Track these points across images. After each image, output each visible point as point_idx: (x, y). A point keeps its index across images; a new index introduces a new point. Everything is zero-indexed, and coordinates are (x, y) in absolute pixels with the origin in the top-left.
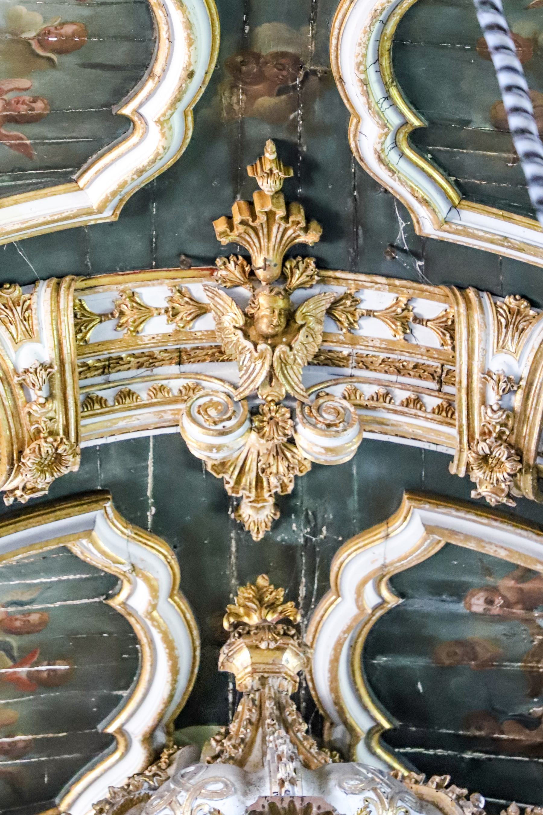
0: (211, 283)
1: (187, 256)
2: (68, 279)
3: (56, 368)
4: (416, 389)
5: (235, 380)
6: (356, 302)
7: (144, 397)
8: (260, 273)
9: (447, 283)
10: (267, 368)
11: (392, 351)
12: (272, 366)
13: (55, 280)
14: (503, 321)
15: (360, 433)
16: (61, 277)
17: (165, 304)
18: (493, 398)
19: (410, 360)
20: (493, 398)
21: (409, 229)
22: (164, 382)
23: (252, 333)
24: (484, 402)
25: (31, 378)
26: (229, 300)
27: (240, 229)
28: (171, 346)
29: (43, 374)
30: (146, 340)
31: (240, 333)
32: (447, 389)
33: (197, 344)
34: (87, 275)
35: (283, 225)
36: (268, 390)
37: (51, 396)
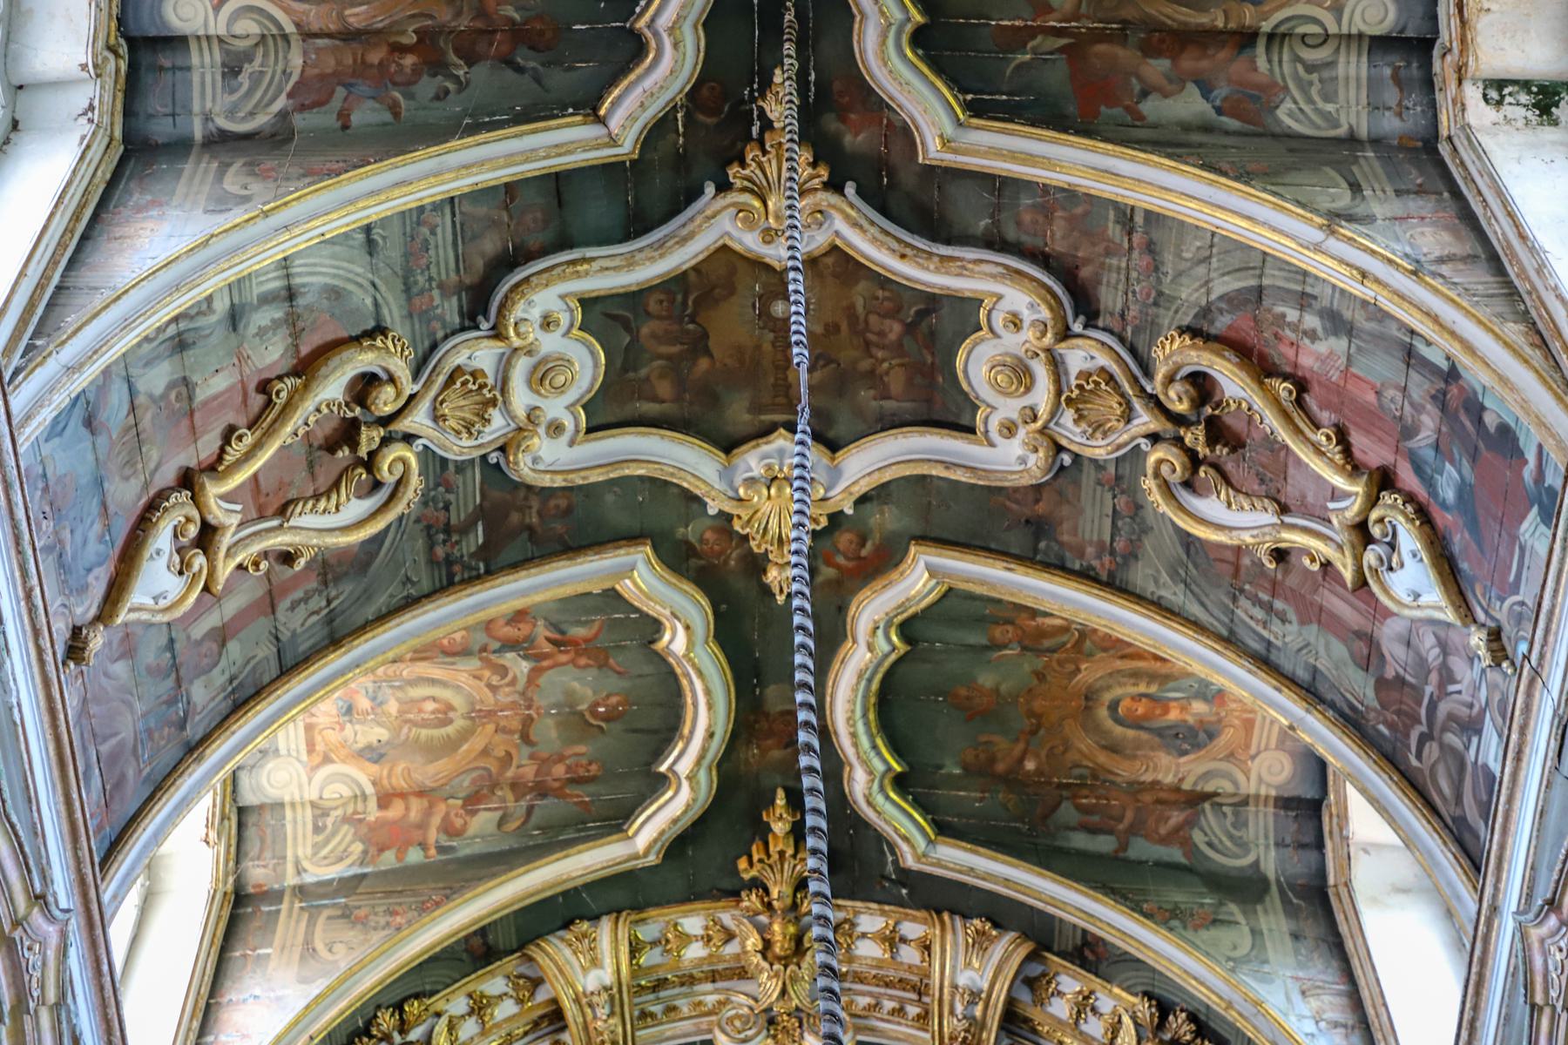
0: (737, 912)
1: (718, 890)
2: (624, 914)
3: (615, 990)
4: (902, 1001)
5: (756, 994)
6: (853, 925)
7: (685, 1010)
8: (775, 903)
9: (927, 908)
10: (780, 983)
11: (880, 968)
12: (784, 984)
13: (615, 915)
14: (970, 940)
15: (854, 1037)
16: (619, 912)
17: (700, 932)
18: (959, 1008)
19: (892, 974)
20: (959, 1008)
21: (896, 862)
22: (702, 998)
23: (769, 955)
24: (952, 1012)
25: (595, 999)
26: (750, 927)
27: (758, 866)
28: (706, 968)
29: (605, 996)
30: (686, 963)
31: (759, 956)
32: (926, 999)
33: (726, 965)
34: (638, 908)
35: (793, 862)
36: (781, 1003)
37: (612, 1014)
